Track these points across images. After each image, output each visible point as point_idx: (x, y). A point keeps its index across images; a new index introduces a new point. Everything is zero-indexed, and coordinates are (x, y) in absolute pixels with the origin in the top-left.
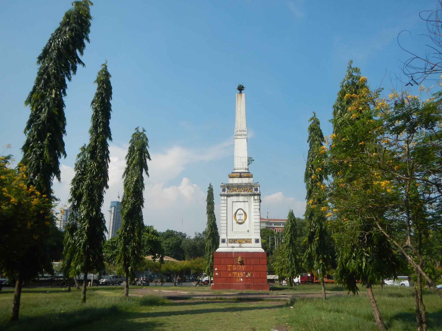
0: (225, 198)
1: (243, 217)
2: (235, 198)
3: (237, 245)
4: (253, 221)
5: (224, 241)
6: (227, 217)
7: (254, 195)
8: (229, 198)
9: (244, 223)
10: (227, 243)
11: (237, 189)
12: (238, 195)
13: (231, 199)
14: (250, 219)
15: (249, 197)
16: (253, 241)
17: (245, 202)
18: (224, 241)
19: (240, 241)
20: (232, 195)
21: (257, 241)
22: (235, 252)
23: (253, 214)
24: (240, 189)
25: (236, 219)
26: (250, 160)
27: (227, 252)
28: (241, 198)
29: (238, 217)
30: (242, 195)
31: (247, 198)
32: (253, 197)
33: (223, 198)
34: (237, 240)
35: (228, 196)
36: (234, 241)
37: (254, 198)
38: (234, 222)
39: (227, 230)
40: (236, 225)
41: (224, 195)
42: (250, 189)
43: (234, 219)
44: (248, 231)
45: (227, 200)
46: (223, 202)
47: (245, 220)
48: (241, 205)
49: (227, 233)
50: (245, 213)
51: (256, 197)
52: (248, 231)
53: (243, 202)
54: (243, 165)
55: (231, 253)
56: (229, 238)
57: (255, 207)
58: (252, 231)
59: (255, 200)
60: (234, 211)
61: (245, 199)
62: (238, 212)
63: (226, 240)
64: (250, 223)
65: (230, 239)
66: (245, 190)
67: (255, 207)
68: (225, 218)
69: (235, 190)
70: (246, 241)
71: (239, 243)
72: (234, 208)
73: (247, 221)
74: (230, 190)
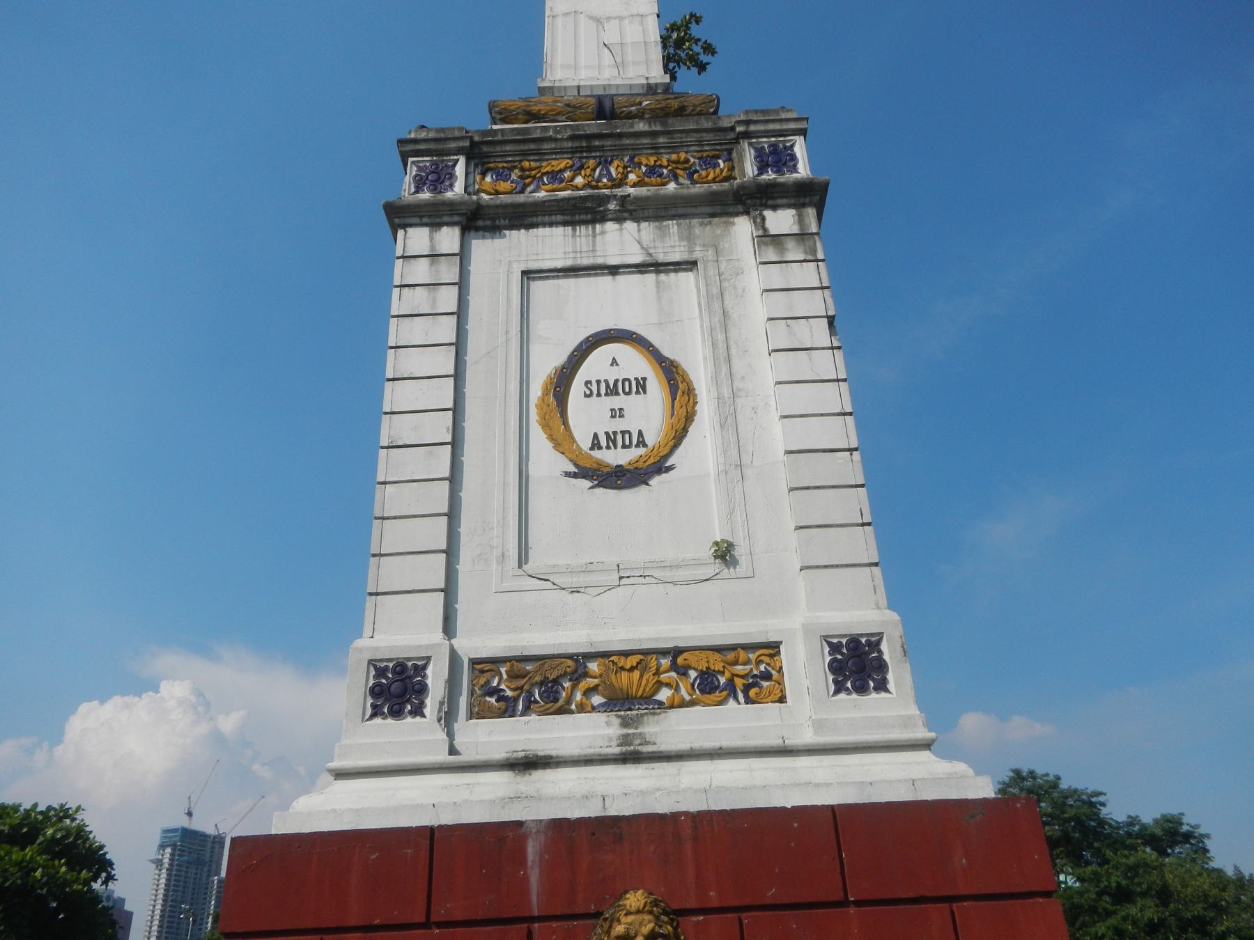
0: (449, 239)
1: (648, 414)
2: (551, 244)
3: (591, 730)
4: (777, 437)
5: (396, 689)
6: (457, 410)
7: (754, 199)
8: (483, 249)
9: (660, 467)
10: (448, 718)
11: (578, 170)
12: (584, 212)
13: (499, 257)
14: (728, 420)
15: (703, 231)
16: (804, 668)
17: (657, 267)
18: (396, 689)
19: (629, 683)
20: (523, 217)
21: (856, 665)
22: (560, 828)
23: (762, 372)
24: (606, 163)
25: (562, 440)
26: (680, 45)
27: (430, 833)
28: (620, 240)
29: (587, 416)
30: (632, 211)
31: (690, 239)
32: (743, 227)
33: (417, 239)
34: (577, 664)
35: (477, 221)
36: (540, 683)
37: (761, 223)
38: (547, 461)
39: (451, 552)
40: (562, 501)
41: (433, 216)
42: (710, 162)
43: (538, 437)
44: (725, 553)
45: (463, 256)
46: (420, 271)
47: (678, 436)
48: (625, 303)
49: (449, 591)
50: (672, 373)
51: (781, 220)
52: (725, 553)
53: (641, 268)
54: (620, 66)
55: (495, 843)
56: (476, 642)
57: (781, 305)
58: (774, 540)
59: (766, 238)
60: (546, 362)
61: (669, 241)
62: (596, 366)
63: (436, 678)
64: (737, 465)
65: (484, 666)
66: (652, 171)
67: (781, 305)
68: (440, 428)
69: (555, 176)
70: (708, 686)
71: (619, 701)
72: (541, 325)
73: (702, 449)
74: (501, 176)
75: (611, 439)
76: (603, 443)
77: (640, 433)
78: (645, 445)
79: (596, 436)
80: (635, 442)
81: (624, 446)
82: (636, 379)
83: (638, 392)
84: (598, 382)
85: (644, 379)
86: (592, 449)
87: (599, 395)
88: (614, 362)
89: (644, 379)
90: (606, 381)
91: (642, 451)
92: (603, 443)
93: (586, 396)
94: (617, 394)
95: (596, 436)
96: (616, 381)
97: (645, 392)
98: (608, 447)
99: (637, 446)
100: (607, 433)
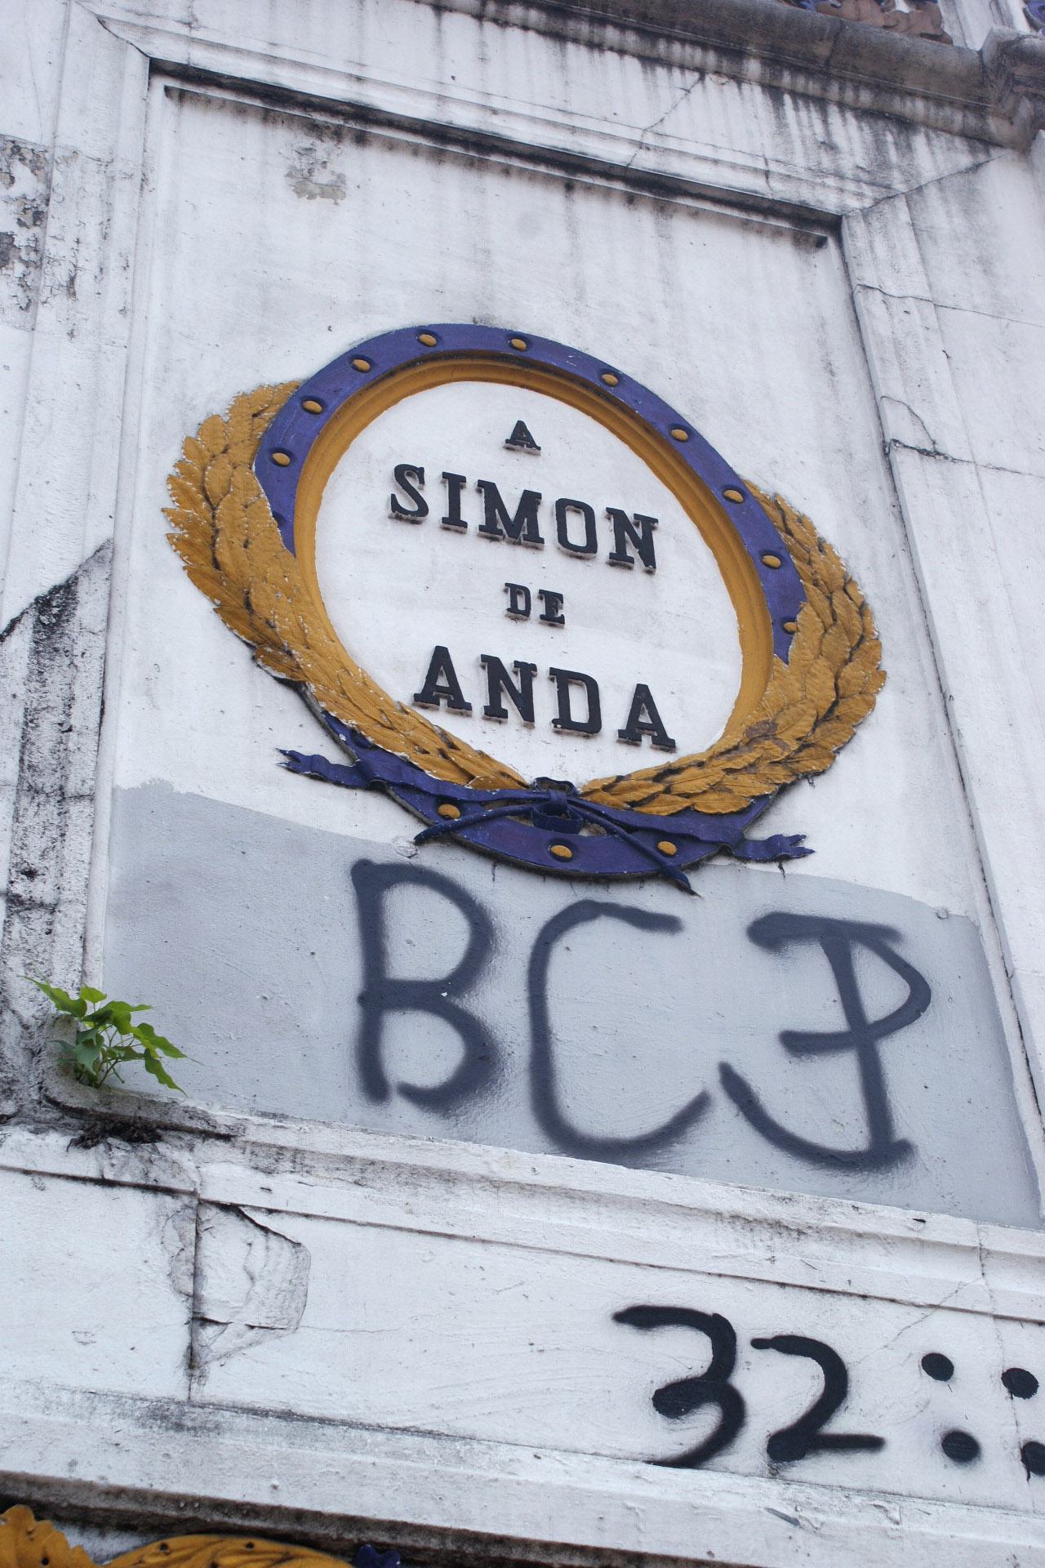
75: (509, 688)
76: (474, 687)
77: (642, 697)
78: (665, 743)
79: (441, 659)
80: (615, 714)
81: (564, 723)
82: (615, 515)
83: (619, 560)
84: (454, 483)
85: (649, 524)
86: (427, 698)
87: (453, 521)
88: (520, 439)
89: (649, 524)
90: (489, 490)
91: (646, 759)
92: (474, 687)
93: (397, 512)
94: (534, 541)
95: (441, 659)
96: (530, 501)
97: (649, 559)
98: (495, 713)
99: (630, 736)
100: (491, 664)
